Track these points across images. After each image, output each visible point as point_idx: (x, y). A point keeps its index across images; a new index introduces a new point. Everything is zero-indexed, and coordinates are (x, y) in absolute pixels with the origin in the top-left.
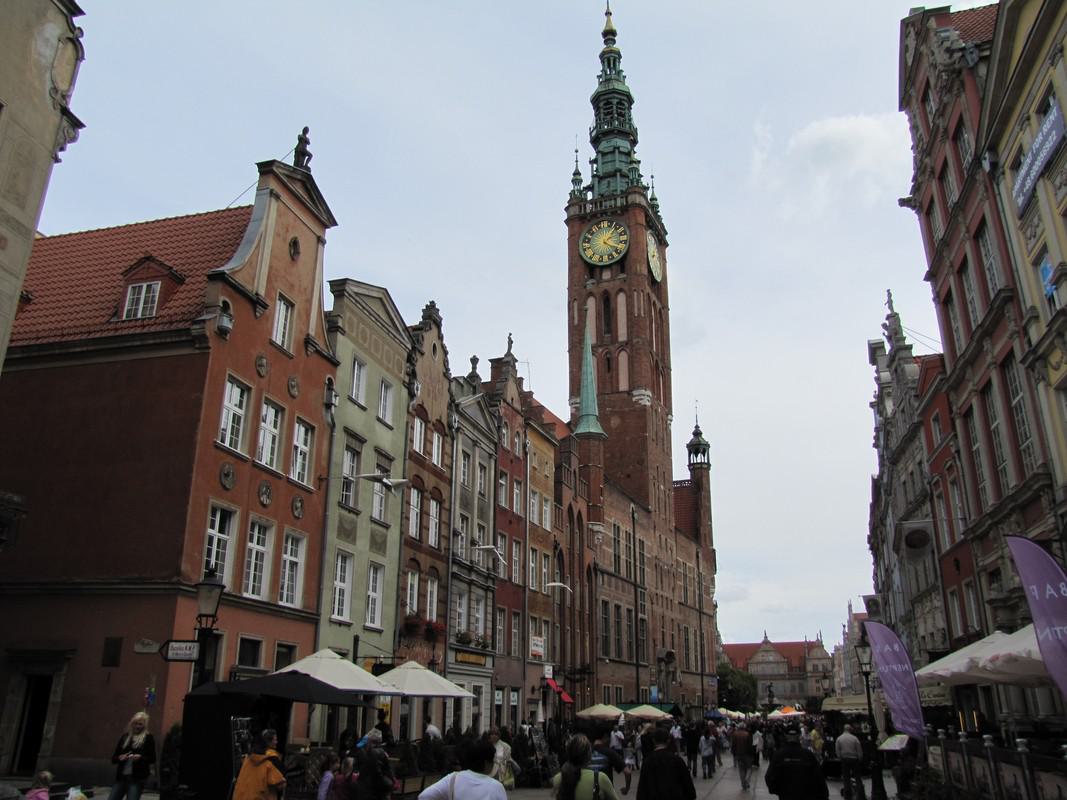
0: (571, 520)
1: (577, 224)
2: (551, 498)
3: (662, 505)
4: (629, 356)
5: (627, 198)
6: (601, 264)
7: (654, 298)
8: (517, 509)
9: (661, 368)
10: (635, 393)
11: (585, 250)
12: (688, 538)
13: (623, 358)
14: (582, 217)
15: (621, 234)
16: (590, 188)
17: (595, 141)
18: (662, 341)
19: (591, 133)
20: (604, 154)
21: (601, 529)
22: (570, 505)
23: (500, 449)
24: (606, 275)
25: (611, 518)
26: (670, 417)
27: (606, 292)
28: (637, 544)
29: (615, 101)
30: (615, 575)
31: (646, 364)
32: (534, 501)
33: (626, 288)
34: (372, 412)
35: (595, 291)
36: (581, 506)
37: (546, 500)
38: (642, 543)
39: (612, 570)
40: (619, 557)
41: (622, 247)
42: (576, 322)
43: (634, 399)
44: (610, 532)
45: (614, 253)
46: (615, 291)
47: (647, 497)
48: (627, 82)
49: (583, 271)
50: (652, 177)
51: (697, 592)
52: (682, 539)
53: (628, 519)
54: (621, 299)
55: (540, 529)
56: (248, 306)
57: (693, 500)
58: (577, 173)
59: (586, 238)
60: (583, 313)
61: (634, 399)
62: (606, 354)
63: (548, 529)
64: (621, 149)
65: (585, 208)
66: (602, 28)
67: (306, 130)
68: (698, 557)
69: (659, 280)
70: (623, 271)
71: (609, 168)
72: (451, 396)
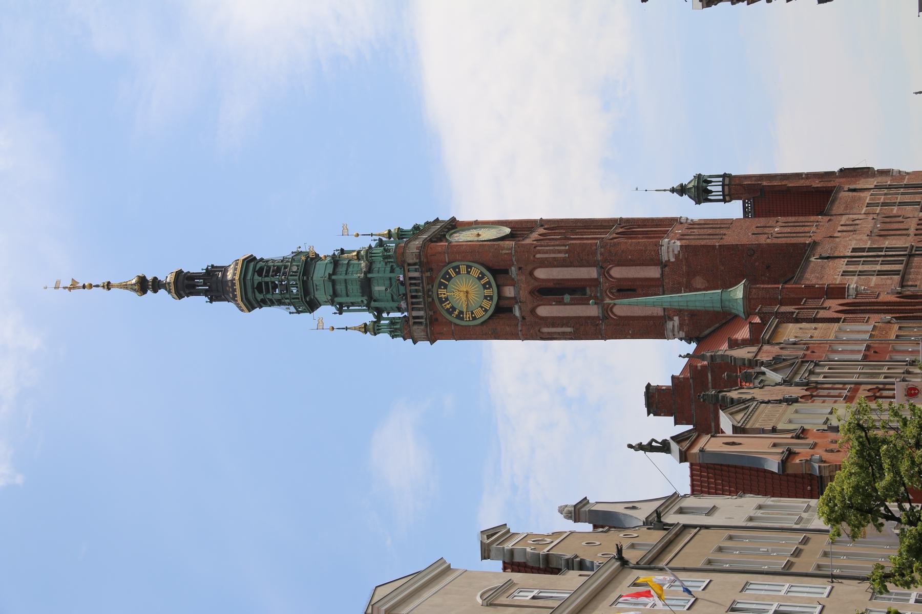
0: (859, 308)
2: (836, 326)
4: (618, 265)
5: (409, 265)
6: (495, 298)
7: (535, 235)
8: (863, 347)
11: (474, 318)
12: (833, 202)
13: (618, 272)
15: (458, 273)
16: (379, 312)
17: (312, 306)
19: (299, 312)
20: (335, 294)
24: (509, 292)
25: (836, 279)
27: (531, 293)
28: (857, 254)
29: (257, 279)
30: (904, 275)
31: (628, 244)
33: (530, 267)
38: (854, 250)
39: (897, 278)
42: (569, 330)
43: (672, 260)
45: (483, 282)
49: (502, 322)
50: (358, 235)
51: (902, 190)
52: (837, 208)
53: (831, 263)
54: (541, 273)
56: (792, 456)
57: (769, 195)
58: (365, 329)
59: (458, 317)
61: (672, 260)
62: (611, 293)
65: (418, 317)
66: (133, 295)
67: (630, 446)
68: (854, 190)
69: (507, 231)
70: (506, 271)
71: (355, 288)
72: (777, 384)
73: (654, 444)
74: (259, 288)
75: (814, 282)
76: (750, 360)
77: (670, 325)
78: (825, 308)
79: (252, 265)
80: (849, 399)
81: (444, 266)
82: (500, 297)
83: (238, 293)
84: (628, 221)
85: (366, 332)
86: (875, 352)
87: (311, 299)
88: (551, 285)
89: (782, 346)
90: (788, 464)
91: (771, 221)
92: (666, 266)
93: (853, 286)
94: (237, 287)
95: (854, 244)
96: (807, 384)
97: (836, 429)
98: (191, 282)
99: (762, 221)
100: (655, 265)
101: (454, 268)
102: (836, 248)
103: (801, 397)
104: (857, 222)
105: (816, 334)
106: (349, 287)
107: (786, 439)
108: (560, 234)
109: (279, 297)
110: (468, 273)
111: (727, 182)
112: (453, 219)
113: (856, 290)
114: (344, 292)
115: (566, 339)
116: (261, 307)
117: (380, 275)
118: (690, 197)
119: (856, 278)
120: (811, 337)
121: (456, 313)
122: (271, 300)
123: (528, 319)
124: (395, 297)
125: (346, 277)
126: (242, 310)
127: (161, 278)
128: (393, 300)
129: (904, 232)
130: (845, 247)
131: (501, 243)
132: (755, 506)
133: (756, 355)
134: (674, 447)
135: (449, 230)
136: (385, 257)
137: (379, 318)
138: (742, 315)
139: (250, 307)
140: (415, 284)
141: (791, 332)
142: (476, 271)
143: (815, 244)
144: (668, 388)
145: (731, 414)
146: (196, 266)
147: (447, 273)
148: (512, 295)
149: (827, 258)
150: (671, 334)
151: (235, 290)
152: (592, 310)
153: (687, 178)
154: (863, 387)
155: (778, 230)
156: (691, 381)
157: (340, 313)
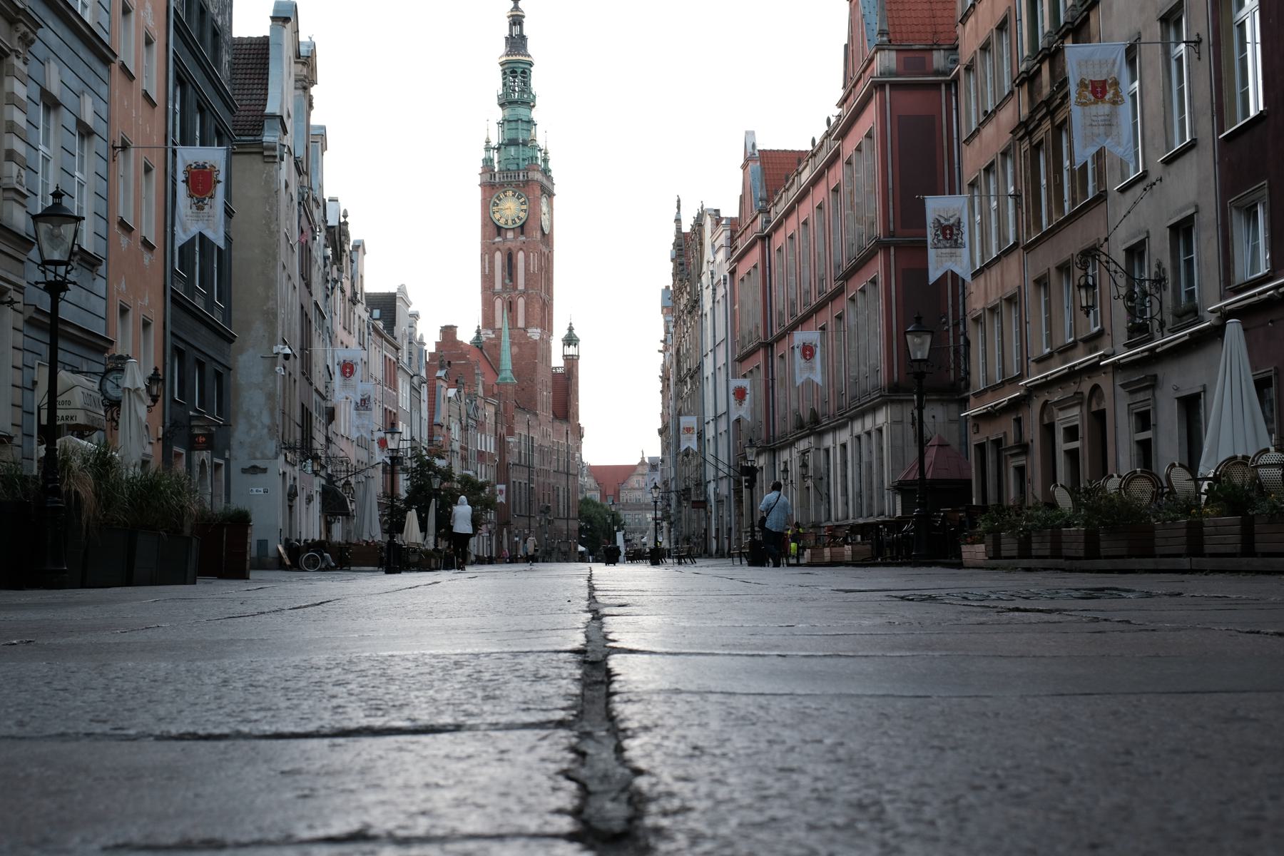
1: (488, 189)
13: (521, 302)
14: (492, 186)
17: (502, 105)
20: (509, 121)
24: (510, 235)
29: (519, 71)
49: (493, 229)
52: (557, 423)
57: (565, 384)
58: (488, 142)
60: (492, 262)
64: (525, 119)
70: (522, 233)
71: (512, 135)
74: (513, 72)
77: (490, 332)
80: (462, 448)
91: (550, 389)
99: (550, 384)
129: (542, 461)
139: (502, 64)
142: (522, 215)
143: (536, 415)
152: (498, 286)
155: (545, 396)
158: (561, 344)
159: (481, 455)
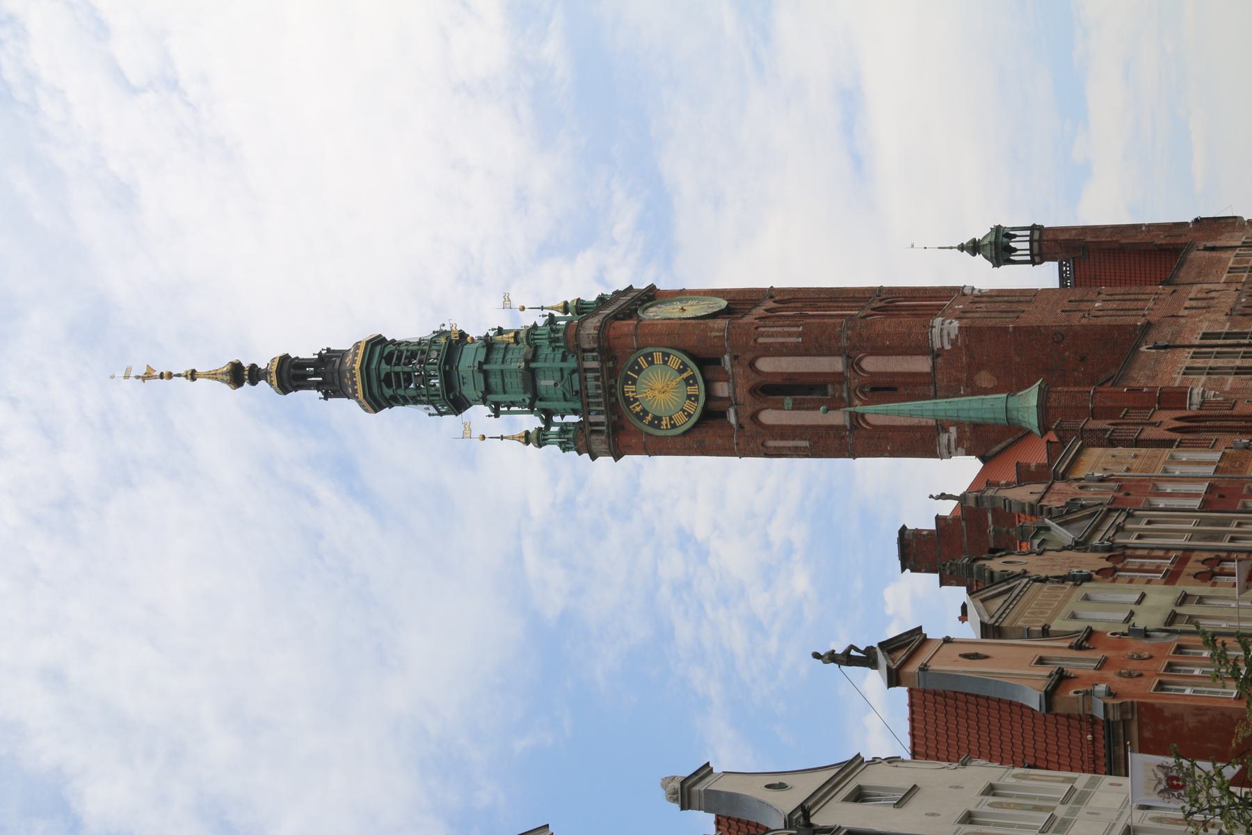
2: (1166, 453)
3: (1128, 305)
4: (872, 354)
5: (585, 351)
7: (759, 311)
8: (1202, 488)
9: (882, 304)
10: (937, 345)
11: (674, 426)
12: (1181, 265)
13: (872, 364)
15: (651, 363)
17: (458, 406)
18: (831, 300)
19: (441, 414)
20: (488, 390)
21: (1198, 391)
22: (1169, 430)
23: (1113, 506)
24: (722, 389)
25: (1174, 379)
26: (966, 291)
27: (752, 391)
29: (385, 368)
31: (885, 325)
32: (1177, 471)
33: (749, 356)
34: (1134, 607)
35: (750, 410)
36: (1167, 417)
37: (1172, 457)
38: (1205, 336)
40: (1238, 368)
41: (676, 360)
42: (805, 444)
43: (948, 347)
44: (1199, 380)
45: (685, 375)
46: (753, 375)
47: (1120, 328)
48: (342, 342)
49: (711, 432)
52: (1183, 275)
53: (1169, 355)
55: (1221, 465)
58: (527, 438)
59: (651, 424)
61: (948, 347)
63: (1216, 456)
64: (481, 358)
65: (597, 424)
67: (816, 656)
68: (1213, 249)
69: (723, 303)
70: (717, 361)
71: (515, 382)
72: (1065, 549)
73: (853, 653)
74: (387, 380)
75: (1142, 382)
76: (1031, 506)
77: (944, 438)
78: (1153, 424)
79: (378, 349)
80: (1171, 578)
81: (631, 354)
82: (709, 395)
83: (359, 387)
84: (891, 290)
85: (527, 443)
86: (1222, 496)
87: (455, 396)
88: (778, 380)
89: (1082, 483)
90: (1057, 698)
92: (938, 356)
93: (1198, 391)
94: (358, 379)
95: (1205, 327)
96: (1110, 549)
97: (1145, 634)
98: (299, 372)
99: (1079, 293)
100: (924, 354)
101: (646, 356)
102: (1179, 332)
103: (1097, 573)
104: (1213, 294)
105: (1136, 463)
106: (507, 380)
107: (1057, 650)
108: (795, 309)
109: (414, 393)
110: (665, 363)
111: (1036, 236)
112: (652, 288)
113: (1203, 396)
114: (500, 387)
115: (799, 456)
116: (391, 406)
117: (547, 365)
118: (986, 257)
119: (1204, 378)
120: (1128, 470)
121: (649, 418)
122: (403, 397)
123: (747, 427)
124: (568, 396)
125: (503, 367)
126: (366, 411)
127: (262, 365)
128: (565, 399)
130: (1193, 331)
131: (711, 323)
132: (982, 786)
133: (1042, 497)
134: (882, 659)
135: (644, 302)
136: (553, 341)
137: (548, 422)
138: (1036, 431)
140: (597, 379)
141: (1096, 461)
144: (930, 531)
145: (983, 601)
146: (306, 350)
147: (637, 363)
148: (726, 394)
149: (1165, 347)
150: (945, 451)
151: (354, 383)
152: (838, 418)
153: (980, 232)
154: (1195, 556)
156: (963, 524)
157: (497, 416)
158: (1006, 269)
159: (1219, 497)
